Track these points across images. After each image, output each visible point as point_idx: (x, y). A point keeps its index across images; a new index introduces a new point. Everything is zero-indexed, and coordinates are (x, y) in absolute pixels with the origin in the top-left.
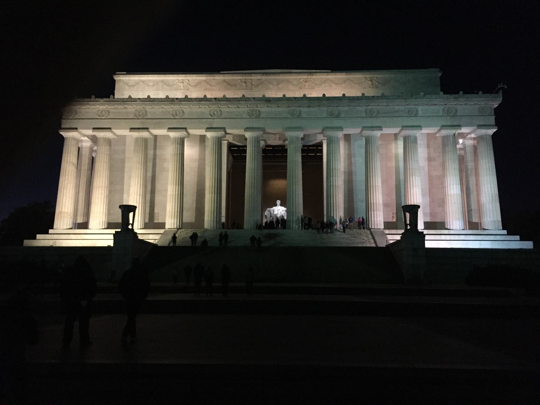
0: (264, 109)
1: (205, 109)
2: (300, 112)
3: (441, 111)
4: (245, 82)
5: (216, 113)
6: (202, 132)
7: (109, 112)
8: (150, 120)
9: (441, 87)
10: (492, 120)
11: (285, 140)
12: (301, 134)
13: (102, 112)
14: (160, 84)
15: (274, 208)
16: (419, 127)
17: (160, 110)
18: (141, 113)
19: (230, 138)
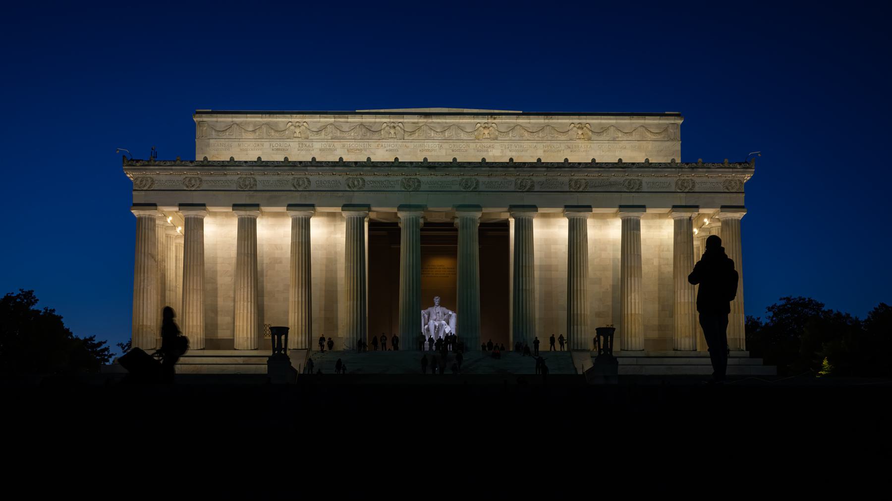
0: (426, 178)
1: (340, 178)
2: (477, 183)
3: (673, 185)
4: (394, 127)
5: (356, 183)
6: (338, 210)
7: (201, 181)
8: (260, 194)
9: (682, 140)
10: (740, 200)
11: (454, 218)
12: (479, 215)
13: (190, 180)
14: (264, 129)
15: (430, 309)
16: (643, 207)
17: (276, 178)
18: (247, 183)
19: (373, 215)
